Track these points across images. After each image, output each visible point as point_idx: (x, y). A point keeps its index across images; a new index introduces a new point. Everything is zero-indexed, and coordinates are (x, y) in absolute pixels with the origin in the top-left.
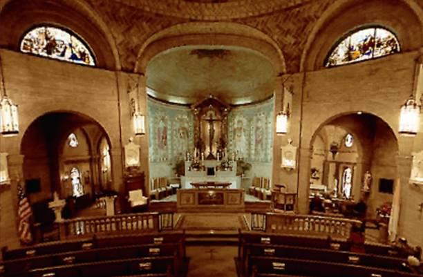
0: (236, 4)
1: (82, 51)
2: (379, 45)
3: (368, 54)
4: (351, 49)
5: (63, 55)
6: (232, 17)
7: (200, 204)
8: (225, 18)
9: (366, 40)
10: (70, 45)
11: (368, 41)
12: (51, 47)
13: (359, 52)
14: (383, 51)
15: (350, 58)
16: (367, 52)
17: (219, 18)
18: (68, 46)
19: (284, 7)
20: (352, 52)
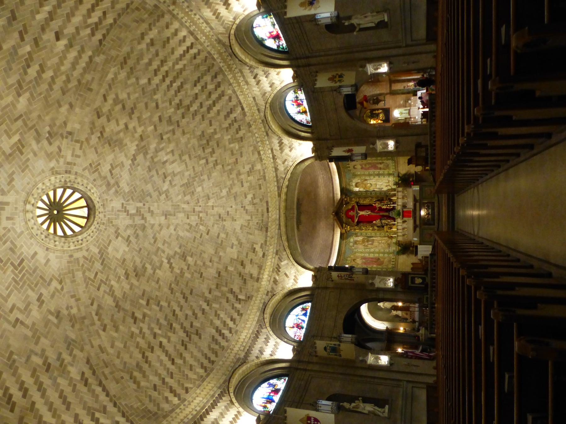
0: (269, 194)
1: (301, 310)
2: (297, 97)
3: (302, 102)
4: (299, 112)
5: (304, 321)
6: (277, 197)
7: (434, 224)
8: (277, 203)
9: (293, 105)
10: (297, 316)
11: (294, 104)
12: (299, 327)
13: (301, 107)
14: (301, 95)
15: (305, 112)
16: (301, 103)
17: (278, 207)
18: (298, 317)
19: (272, 160)
20: (301, 111)
